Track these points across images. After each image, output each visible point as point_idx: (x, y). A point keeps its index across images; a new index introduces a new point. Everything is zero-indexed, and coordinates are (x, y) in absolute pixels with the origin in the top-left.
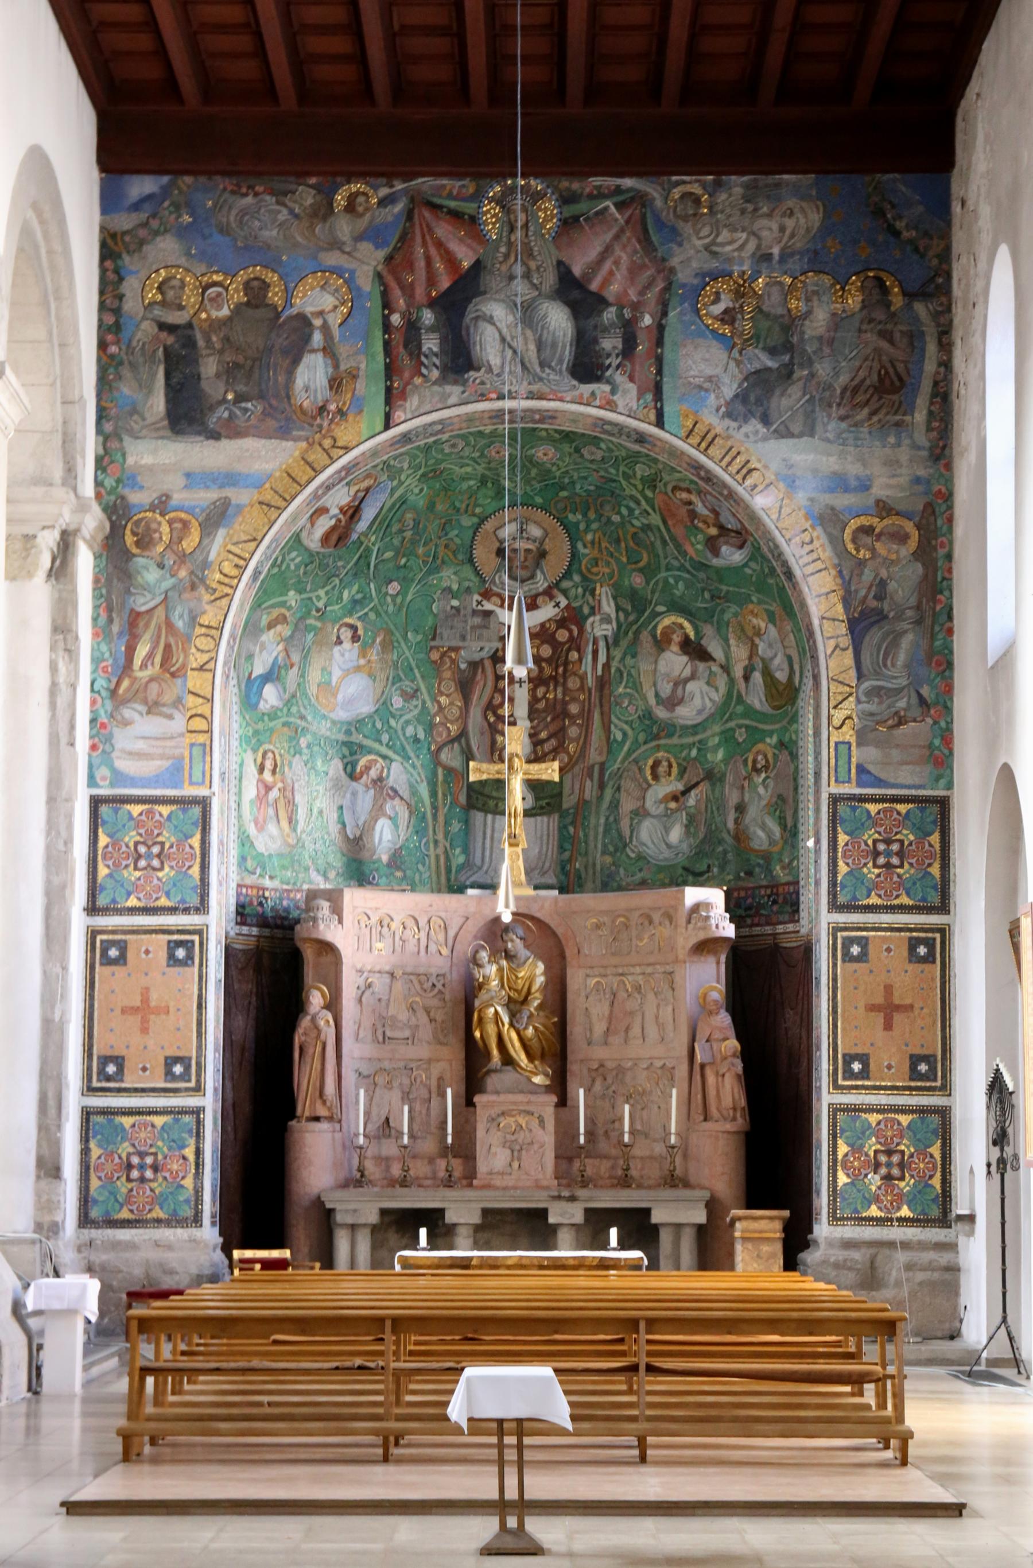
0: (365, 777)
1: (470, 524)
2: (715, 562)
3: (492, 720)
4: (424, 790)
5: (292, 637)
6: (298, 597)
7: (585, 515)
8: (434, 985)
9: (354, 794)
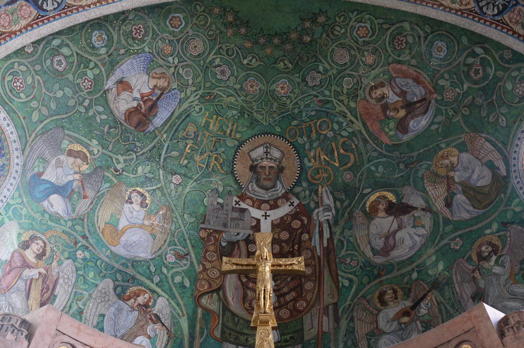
0: (132, 300)
1: (232, 145)
2: (406, 138)
3: (244, 280)
4: (184, 324)
5: (89, 175)
6: (100, 148)
7: (309, 137)
9: (120, 310)
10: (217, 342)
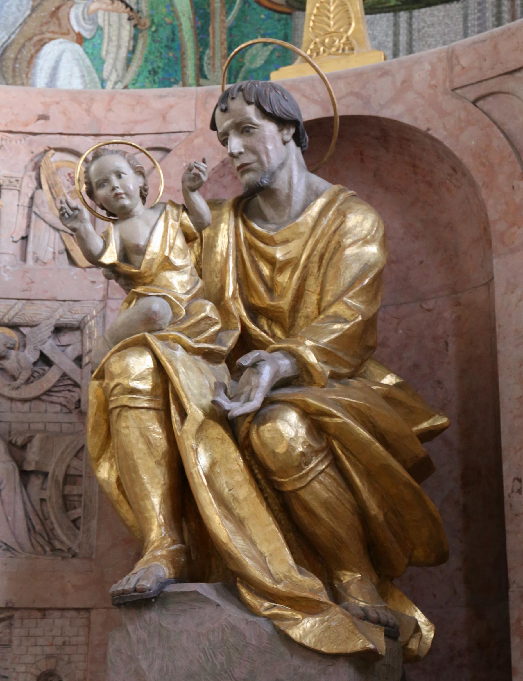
8: (45, 360)
10: (277, 16)
